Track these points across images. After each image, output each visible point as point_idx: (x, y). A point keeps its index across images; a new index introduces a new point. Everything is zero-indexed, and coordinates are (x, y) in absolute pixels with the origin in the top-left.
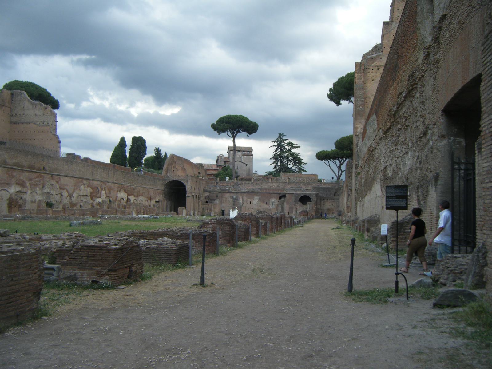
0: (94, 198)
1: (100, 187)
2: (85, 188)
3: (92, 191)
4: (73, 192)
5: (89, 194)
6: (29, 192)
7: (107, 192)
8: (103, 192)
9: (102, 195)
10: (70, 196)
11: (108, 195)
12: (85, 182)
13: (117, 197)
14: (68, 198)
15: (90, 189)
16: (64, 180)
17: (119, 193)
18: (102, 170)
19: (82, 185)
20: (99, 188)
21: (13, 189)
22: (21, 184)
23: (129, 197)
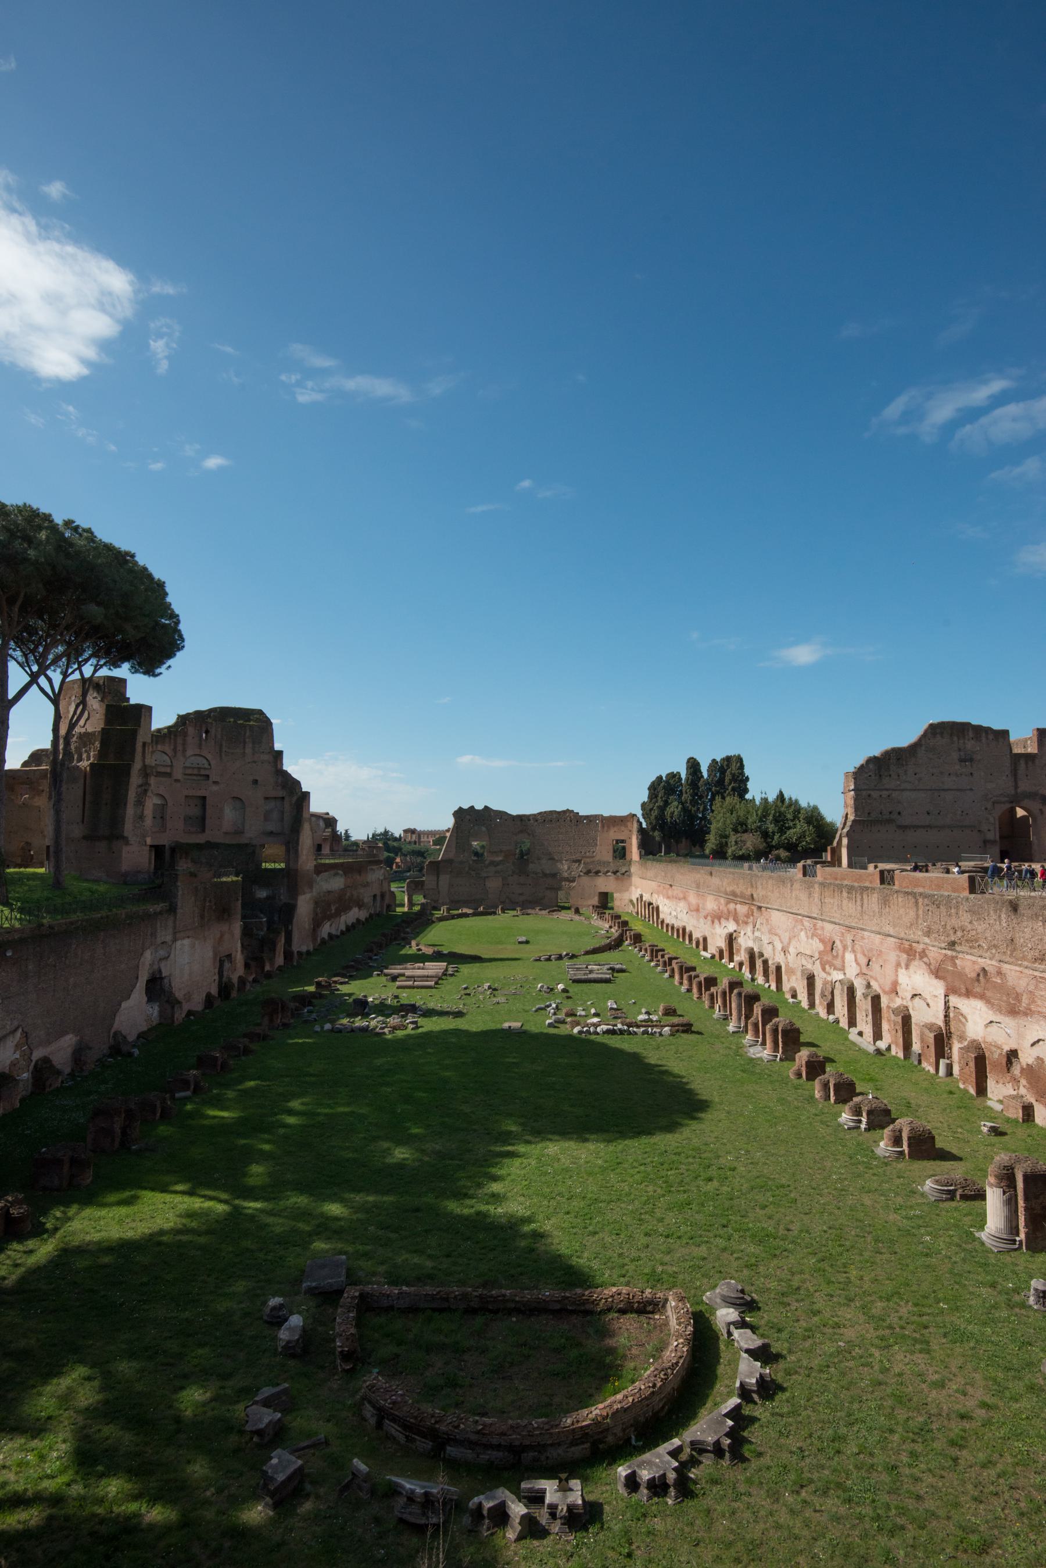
0: (827, 967)
1: (841, 941)
2: (807, 937)
3: (821, 947)
4: (789, 944)
5: (817, 955)
6: (742, 933)
7: (863, 961)
8: (849, 957)
9: (846, 965)
10: (785, 951)
11: (865, 970)
12: (807, 923)
13: (895, 984)
14: (782, 954)
15: (818, 941)
16: (776, 917)
17: (902, 972)
18: (845, 894)
19: (802, 930)
20: (838, 943)
21: (731, 927)
22: (736, 920)
23: (954, 1000)
